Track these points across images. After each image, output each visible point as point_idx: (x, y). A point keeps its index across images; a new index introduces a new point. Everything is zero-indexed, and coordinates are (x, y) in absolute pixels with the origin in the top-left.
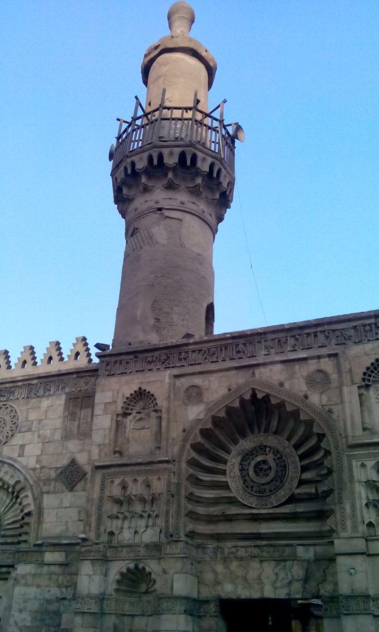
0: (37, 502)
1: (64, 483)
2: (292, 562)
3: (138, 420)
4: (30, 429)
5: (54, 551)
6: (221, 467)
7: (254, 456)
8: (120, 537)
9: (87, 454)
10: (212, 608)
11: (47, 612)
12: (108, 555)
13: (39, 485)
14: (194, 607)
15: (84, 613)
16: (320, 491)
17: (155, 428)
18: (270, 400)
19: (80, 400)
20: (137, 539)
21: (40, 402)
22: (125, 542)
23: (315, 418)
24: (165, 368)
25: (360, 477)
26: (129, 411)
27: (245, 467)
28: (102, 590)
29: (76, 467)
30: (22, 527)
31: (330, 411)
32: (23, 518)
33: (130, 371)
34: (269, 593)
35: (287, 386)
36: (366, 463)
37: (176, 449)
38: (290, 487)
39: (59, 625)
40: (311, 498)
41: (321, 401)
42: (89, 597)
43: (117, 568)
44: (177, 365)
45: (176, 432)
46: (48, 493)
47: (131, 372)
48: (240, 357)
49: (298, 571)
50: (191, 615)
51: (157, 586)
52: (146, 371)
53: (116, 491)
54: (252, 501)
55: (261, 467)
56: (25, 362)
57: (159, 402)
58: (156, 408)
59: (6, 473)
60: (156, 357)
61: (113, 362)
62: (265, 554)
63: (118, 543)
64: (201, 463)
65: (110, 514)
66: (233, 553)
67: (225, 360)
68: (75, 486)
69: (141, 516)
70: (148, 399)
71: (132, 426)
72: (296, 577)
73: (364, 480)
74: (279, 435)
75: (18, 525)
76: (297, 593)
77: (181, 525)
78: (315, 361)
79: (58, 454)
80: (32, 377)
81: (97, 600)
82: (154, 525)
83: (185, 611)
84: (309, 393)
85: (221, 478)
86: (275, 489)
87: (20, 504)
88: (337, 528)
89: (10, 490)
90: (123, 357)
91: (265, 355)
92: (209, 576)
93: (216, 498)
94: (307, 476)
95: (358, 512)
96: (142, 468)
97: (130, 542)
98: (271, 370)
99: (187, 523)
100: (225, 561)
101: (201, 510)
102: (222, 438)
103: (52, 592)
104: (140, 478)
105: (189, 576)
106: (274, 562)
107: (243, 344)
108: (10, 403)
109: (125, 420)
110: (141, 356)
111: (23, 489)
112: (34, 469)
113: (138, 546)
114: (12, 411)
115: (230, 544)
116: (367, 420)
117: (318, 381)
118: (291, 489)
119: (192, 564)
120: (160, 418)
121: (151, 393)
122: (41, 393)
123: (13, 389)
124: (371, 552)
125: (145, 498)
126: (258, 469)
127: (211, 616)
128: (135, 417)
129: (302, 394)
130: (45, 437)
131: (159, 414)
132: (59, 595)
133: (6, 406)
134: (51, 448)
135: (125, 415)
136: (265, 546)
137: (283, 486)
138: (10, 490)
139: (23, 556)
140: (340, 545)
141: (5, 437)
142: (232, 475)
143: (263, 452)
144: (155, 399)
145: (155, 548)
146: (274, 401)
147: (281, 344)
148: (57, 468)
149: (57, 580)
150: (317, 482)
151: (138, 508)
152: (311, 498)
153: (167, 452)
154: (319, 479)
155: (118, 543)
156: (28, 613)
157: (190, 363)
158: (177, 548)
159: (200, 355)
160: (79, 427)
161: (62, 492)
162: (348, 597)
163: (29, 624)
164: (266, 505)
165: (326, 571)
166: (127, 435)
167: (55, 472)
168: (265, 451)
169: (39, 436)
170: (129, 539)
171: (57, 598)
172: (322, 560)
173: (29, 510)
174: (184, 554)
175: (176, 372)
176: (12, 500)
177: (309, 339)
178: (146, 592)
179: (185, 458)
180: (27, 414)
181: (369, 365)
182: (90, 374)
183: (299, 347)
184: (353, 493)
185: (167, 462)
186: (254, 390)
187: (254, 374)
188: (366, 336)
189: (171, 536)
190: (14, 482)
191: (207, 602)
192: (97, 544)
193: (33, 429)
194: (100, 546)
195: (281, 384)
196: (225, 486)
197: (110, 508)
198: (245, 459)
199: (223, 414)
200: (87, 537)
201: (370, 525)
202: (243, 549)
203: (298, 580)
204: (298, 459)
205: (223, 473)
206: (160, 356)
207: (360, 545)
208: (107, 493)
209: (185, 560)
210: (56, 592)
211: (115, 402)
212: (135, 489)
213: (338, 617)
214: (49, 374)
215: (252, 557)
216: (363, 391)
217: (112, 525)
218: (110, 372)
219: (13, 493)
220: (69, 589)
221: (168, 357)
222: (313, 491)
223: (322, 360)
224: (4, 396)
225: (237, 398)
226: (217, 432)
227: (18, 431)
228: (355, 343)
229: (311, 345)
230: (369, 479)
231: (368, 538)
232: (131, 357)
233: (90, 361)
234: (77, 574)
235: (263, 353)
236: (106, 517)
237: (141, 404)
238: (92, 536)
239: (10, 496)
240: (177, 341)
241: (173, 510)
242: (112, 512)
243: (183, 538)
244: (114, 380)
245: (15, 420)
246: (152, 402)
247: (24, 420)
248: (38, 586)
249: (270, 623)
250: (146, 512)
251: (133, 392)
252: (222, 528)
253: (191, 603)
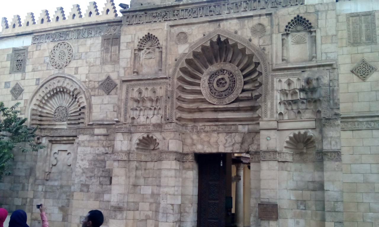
0: (88, 101)
1: (104, 90)
2: (235, 134)
3: (148, 53)
4: (80, 58)
5: (99, 128)
6: (197, 81)
7: (217, 75)
8: (138, 120)
9: (117, 73)
10: (191, 157)
11: (98, 160)
12: (132, 130)
13: (89, 91)
14: (181, 157)
15: (118, 160)
16: (254, 95)
17: (158, 59)
18: (228, 42)
19: (111, 40)
20: (148, 122)
21: (86, 41)
22: (141, 123)
23: (255, 53)
24: (164, 21)
25: (277, 88)
26: (142, 48)
27: (211, 82)
28: (129, 148)
29: (110, 81)
30: (80, 115)
31: (264, 49)
32: (80, 110)
33: (142, 22)
34: (222, 150)
35: (239, 33)
37: (171, 71)
38: (237, 93)
39: (105, 167)
40: (249, 99)
41: (259, 43)
42: (121, 152)
43: (137, 137)
44: (172, 19)
45: (171, 61)
46: (94, 96)
47: (143, 23)
48: (211, 14)
49: (238, 138)
50: (179, 161)
51: (159, 146)
52: (152, 22)
53: (136, 95)
54: (215, 101)
55: (221, 81)
56: (74, 15)
57: (160, 42)
58: (159, 46)
59: (68, 84)
60: (159, 14)
61: (131, 16)
62: (220, 129)
63: (137, 123)
64: (185, 79)
65: (132, 108)
66: (202, 129)
67: (202, 16)
68: (110, 92)
69: (150, 109)
70: (154, 40)
71: (144, 57)
72: (237, 141)
73: (279, 89)
74: (232, 63)
75: (77, 114)
76: (237, 150)
77: (174, 114)
78: (258, 18)
79: (99, 73)
80: (79, 25)
81: (126, 153)
82: (158, 114)
83: (175, 159)
84: (252, 38)
85: (197, 88)
86: (228, 94)
87: (78, 102)
88: (262, 115)
89: (71, 94)
90: (137, 13)
91: (227, 13)
92: (189, 141)
93: (194, 99)
94: (247, 87)
95: (275, 107)
96: (151, 82)
97: (144, 123)
98: (230, 23)
99: (177, 113)
100: (198, 133)
101: (185, 106)
102: (198, 64)
103: (100, 150)
104: (149, 87)
105: (177, 141)
106: (225, 134)
107: (213, 6)
108: (66, 41)
109: (139, 53)
110: (149, 12)
111: (79, 93)
112: (85, 82)
113: (149, 125)
114: (68, 46)
115: (201, 124)
116: (285, 55)
117: (259, 30)
118: (237, 94)
119: (179, 135)
120: (161, 52)
121: (156, 37)
122: (86, 35)
123: (68, 33)
124: (279, 129)
125: (152, 99)
126: (219, 83)
127: (189, 162)
128: (146, 51)
129: (248, 39)
130: (90, 62)
131: (160, 50)
132: (104, 151)
133: (65, 43)
134: (94, 69)
135: (140, 50)
136: (221, 125)
137: (233, 92)
138: (71, 94)
139: (83, 131)
140: (263, 124)
141: (65, 62)
142: (204, 86)
143: (223, 73)
144: (158, 40)
145: (159, 127)
146: (231, 43)
147: (237, 6)
148: (99, 82)
149: (103, 143)
150: (252, 90)
151: (149, 104)
152: (249, 99)
153: (166, 72)
154: (254, 89)
155: (137, 123)
156: (87, 161)
157: (180, 18)
158: (171, 126)
159: (186, 13)
160: (111, 57)
161: (103, 95)
162: (265, 152)
163: (87, 167)
164: (223, 103)
165: (254, 139)
166: (141, 63)
167: (98, 84)
168: (224, 72)
169: (87, 62)
170: (144, 121)
171: (103, 153)
172: (252, 132)
173: (84, 105)
174: (175, 129)
175: (171, 23)
176: (72, 99)
177: (255, 3)
178: (154, 149)
179: (176, 76)
180: (78, 48)
181: (290, 21)
182: (117, 24)
183: (249, 9)
184: (272, 97)
185: (166, 78)
186: (219, 36)
187: (219, 25)
188: (290, 3)
189: (168, 120)
190: (73, 89)
191: (187, 154)
192: (125, 124)
193: (82, 58)
194: (127, 125)
195: (236, 32)
196: (200, 93)
197: (132, 104)
198: (211, 77)
199: (199, 50)
200: (119, 120)
201: (281, 114)
203: (238, 143)
204: (242, 77)
205: (199, 85)
206: (161, 12)
207: (274, 124)
208: (130, 96)
209: (176, 132)
210: (102, 150)
211: (133, 42)
212: (147, 94)
213: (259, 162)
214: (90, 23)
215: (213, 131)
216: (284, 37)
217: (134, 114)
218: (129, 23)
219: (73, 95)
220: (109, 148)
221: (166, 14)
222: (250, 95)
223: (262, 17)
224: (63, 37)
225: (209, 40)
226: (196, 61)
227: (73, 59)
228: (283, 7)
229: (256, 7)
230: (283, 89)
231: (279, 121)
232: (143, 13)
233: (116, 15)
234: (114, 140)
235: (226, 12)
236: (130, 109)
237: (149, 43)
238: (122, 119)
239: (72, 97)
240: (172, 3)
242: (133, 106)
243: (175, 121)
244: (132, 28)
245: (71, 52)
246: (156, 42)
247: (77, 52)
248: (92, 147)
249: (221, 165)
250: (153, 106)
251: (144, 36)
252: (197, 116)
253: (179, 155)
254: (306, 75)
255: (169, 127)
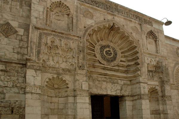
36: (149, 59)
55: (108, 52)
94: (123, 59)
142: (97, 52)
186: (114, 24)
189: (80, 67)
202: (100, 78)
241: (81, 56)
254: (157, 59)
255: (81, 72)
